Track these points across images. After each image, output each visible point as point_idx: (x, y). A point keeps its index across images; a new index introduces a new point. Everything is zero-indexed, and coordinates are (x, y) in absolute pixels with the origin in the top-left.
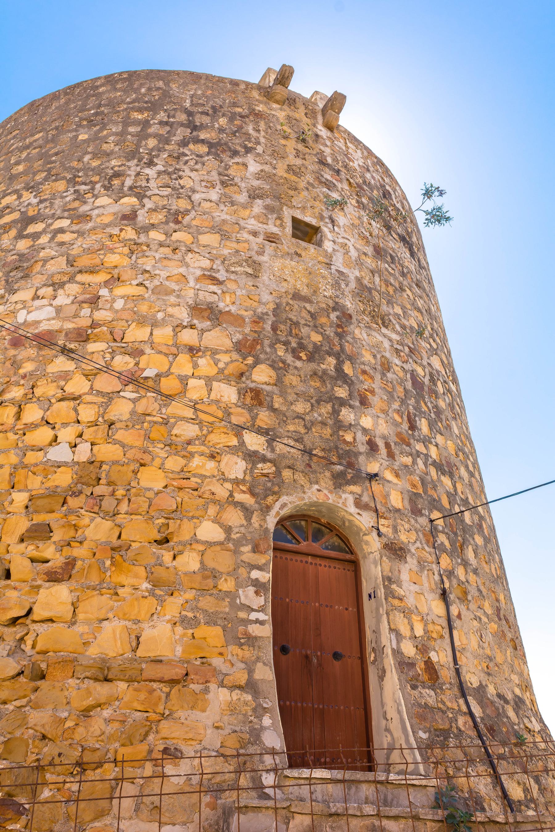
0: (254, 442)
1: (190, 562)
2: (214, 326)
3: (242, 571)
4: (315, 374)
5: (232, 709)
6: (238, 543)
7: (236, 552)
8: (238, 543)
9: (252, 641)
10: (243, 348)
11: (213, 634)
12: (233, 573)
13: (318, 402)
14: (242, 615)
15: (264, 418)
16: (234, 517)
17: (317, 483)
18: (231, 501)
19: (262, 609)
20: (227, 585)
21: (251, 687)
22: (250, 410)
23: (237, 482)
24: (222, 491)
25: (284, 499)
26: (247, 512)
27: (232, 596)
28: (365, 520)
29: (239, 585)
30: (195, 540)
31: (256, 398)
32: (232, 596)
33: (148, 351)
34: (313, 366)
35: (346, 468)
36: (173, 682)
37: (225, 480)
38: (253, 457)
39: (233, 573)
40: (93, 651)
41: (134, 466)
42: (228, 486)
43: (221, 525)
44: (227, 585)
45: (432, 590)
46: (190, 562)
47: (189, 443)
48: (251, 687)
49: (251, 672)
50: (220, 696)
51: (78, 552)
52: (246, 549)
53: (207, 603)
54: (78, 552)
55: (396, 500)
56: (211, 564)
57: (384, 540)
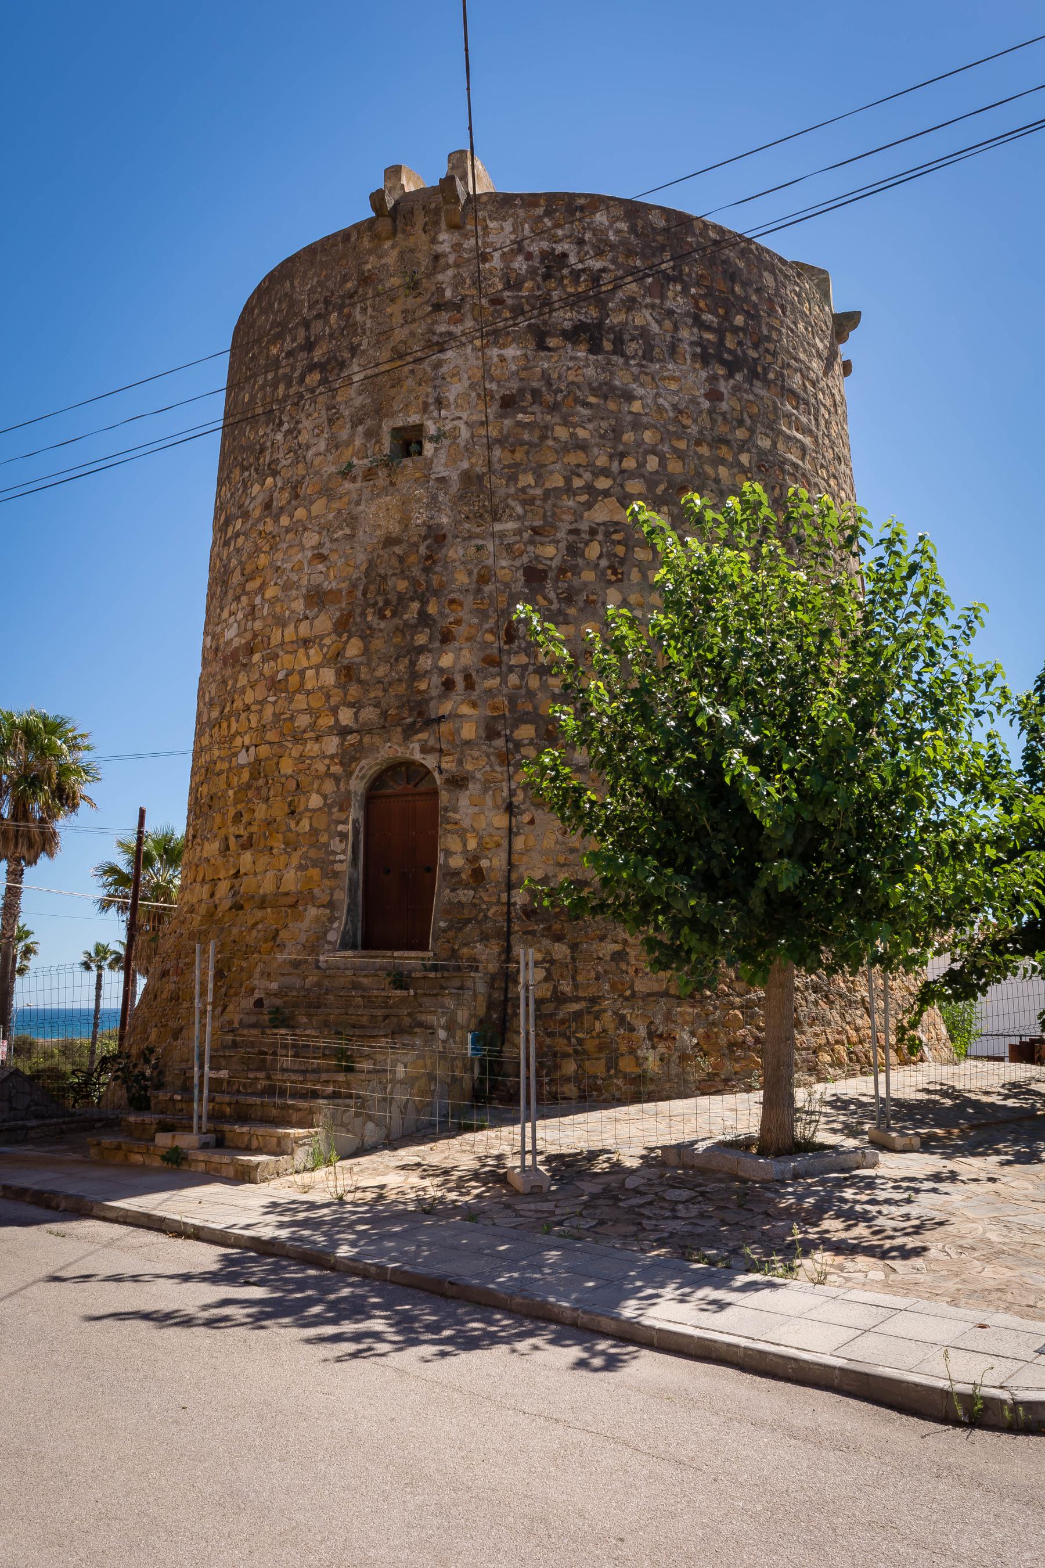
0: (346, 717)
1: (305, 825)
2: (320, 611)
3: (332, 827)
4: (397, 629)
5: (317, 919)
6: (330, 806)
7: (330, 813)
8: (330, 806)
9: (336, 875)
10: (342, 626)
11: (315, 872)
12: (327, 829)
13: (396, 660)
14: (332, 858)
15: (354, 690)
16: (329, 786)
17: (389, 740)
18: (328, 774)
19: (344, 852)
20: (323, 838)
21: (331, 905)
22: (344, 687)
23: (332, 757)
24: (321, 767)
25: (363, 762)
26: (337, 779)
27: (327, 845)
28: (430, 762)
29: (331, 837)
30: (307, 809)
31: (347, 673)
32: (327, 845)
33: (281, 653)
34: (396, 621)
35: (419, 717)
36: (290, 906)
37: (325, 757)
38: (344, 732)
39: (327, 829)
40: (261, 891)
41: (275, 760)
42: (327, 761)
43: (321, 795)
44: (323, 838)
45: (496, 807)
46: (305, 825)
47: (304, 731)
48: (331, 905)
49: (332, 895)
50: (313, 912)
51: (254, 829)
52: (335, 809)
53: (312, 853)
54: (254, 829)
55: (468, 731)
56: (315, 825)
57: (445, 775)
